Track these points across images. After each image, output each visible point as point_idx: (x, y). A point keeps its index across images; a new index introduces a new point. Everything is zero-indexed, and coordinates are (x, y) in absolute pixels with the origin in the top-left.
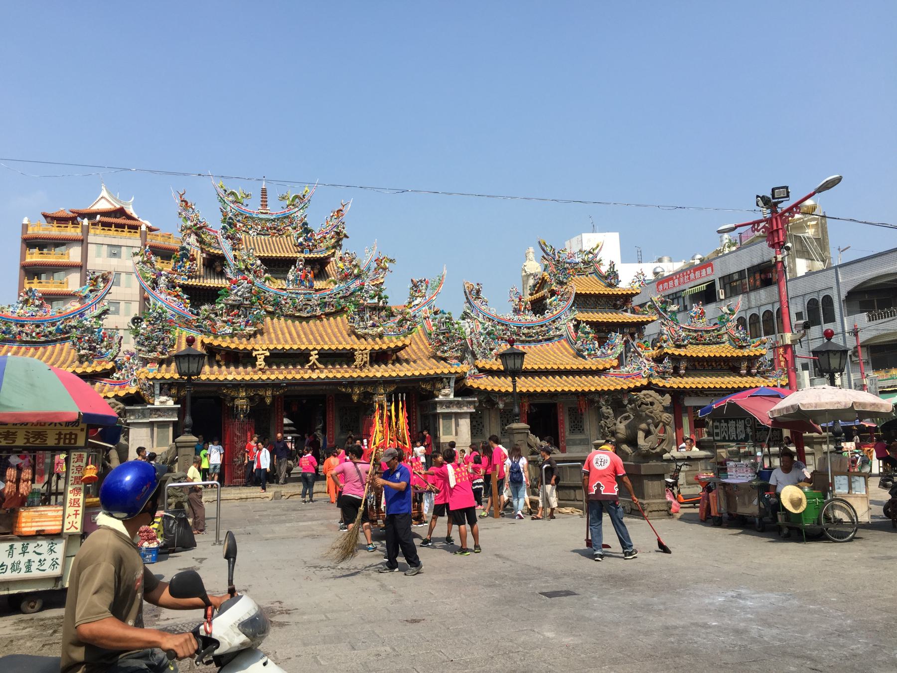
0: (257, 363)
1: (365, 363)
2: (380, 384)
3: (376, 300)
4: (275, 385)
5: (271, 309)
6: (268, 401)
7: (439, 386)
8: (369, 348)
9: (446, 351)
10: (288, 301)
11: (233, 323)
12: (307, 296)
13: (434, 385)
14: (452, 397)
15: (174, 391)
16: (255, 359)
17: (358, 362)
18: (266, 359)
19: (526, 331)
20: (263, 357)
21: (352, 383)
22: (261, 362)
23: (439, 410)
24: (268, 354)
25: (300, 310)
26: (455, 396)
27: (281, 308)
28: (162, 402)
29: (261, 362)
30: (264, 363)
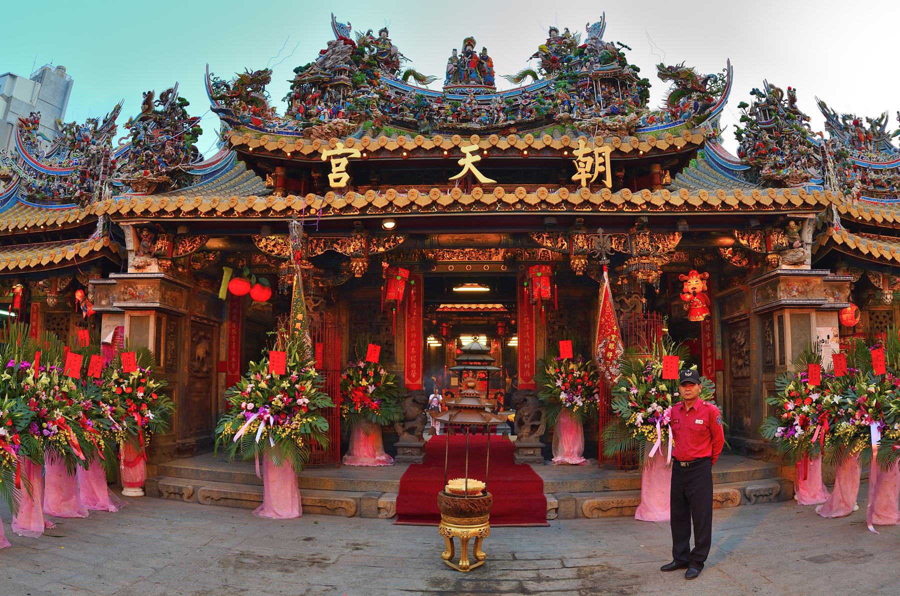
0: (331, 177)
1: (602, 175)
2: (641, 228)
3: (615, 65)
4: (369, 226)
5: (410, 117)
6: (358, 266)
9: (782, 167)
10: (447, 106)
11: (308, 116)
12: (482, 97)
13: (766, 241)
16: (326, 167)
17: (582, 176)
18: (354, 167)
20: (344, 162)
21: (566, 224)
22: (339, 176)
23: (784, 298)
24: (357, 154)
25: (465, 120)
26: (814, 267)
27: (430, 119)
28: (138, 268)
29: (339, 176)
30: (346, 177)
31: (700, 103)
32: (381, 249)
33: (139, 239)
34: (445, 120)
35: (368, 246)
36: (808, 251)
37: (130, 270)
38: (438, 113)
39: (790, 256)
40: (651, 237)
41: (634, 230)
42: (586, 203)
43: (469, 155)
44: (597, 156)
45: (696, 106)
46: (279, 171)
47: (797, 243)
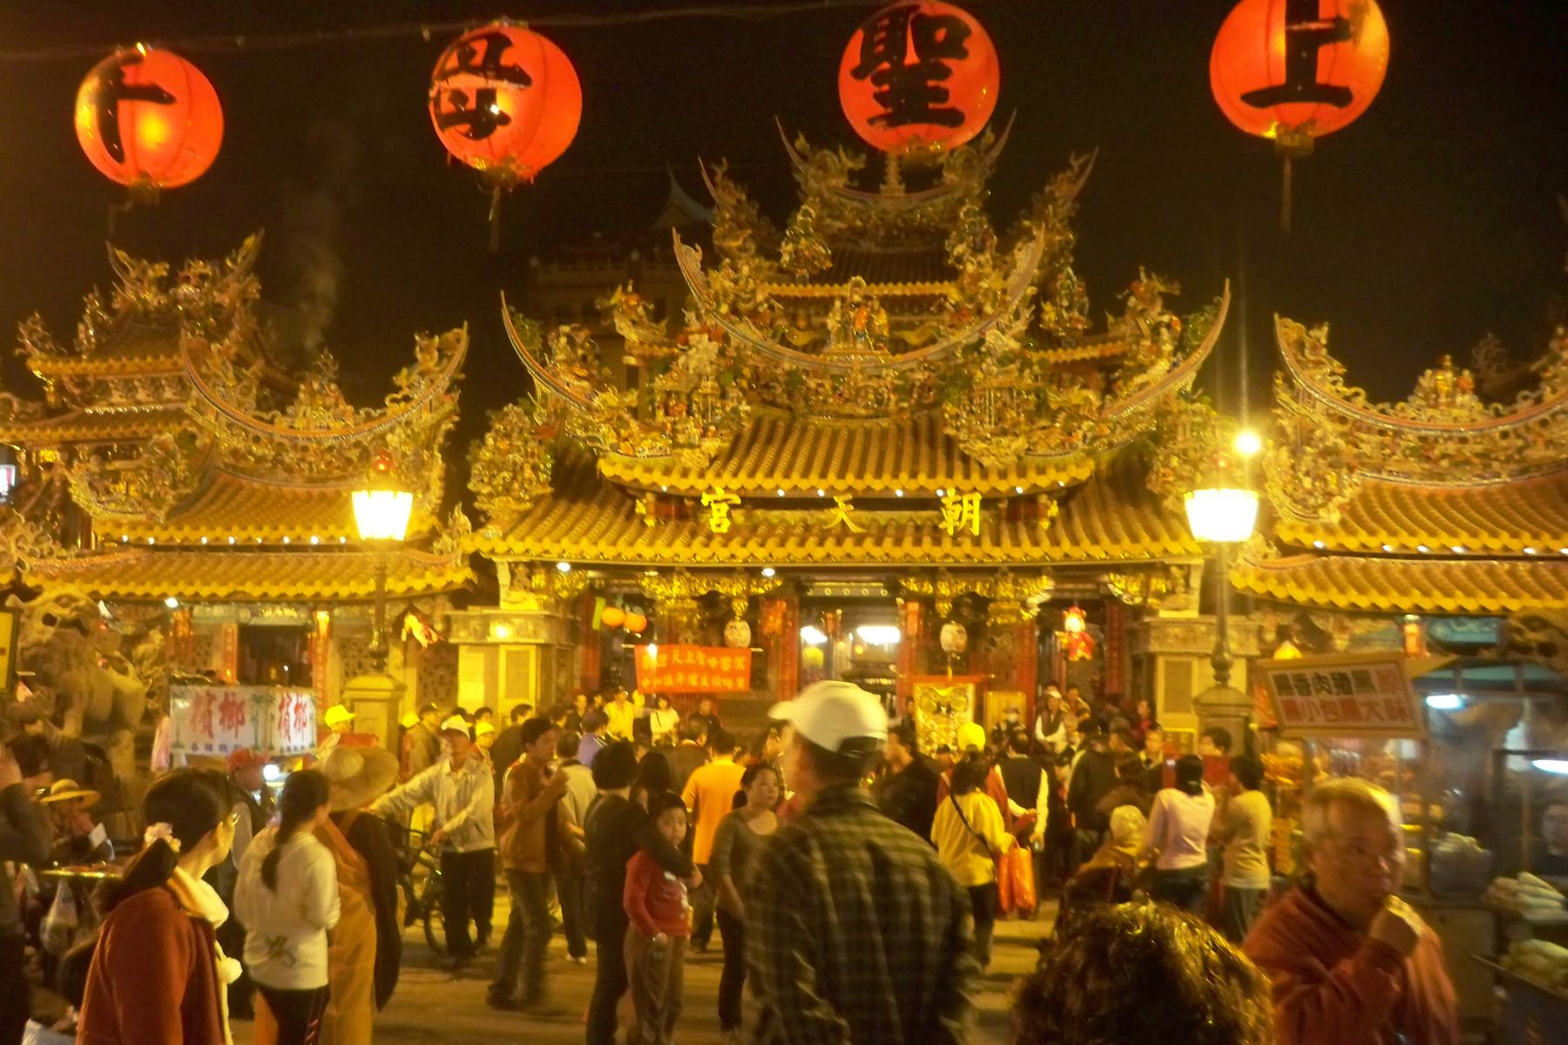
7: (1159, 584)
8: (984, 486)
14: (1193, 613)
15: (539, 580)
19: (1451, 448)
21: (931, 573)
23: (1154, 647)
31: (1089, 435)
32: (761, 591)
33: (513, 574)
34: (825, 402)
35: (749, 587)
36: (1195, 597)
37: (503, 604)
38: (817, 393)
39: (1170, 600)
40: (1015, 583)
41: (998, 576)
42: (947, 556)
43: (841, 504)
44: (965, 502)
45: (1085, 437)
46: (650, 497)
47: (1180, 589)
